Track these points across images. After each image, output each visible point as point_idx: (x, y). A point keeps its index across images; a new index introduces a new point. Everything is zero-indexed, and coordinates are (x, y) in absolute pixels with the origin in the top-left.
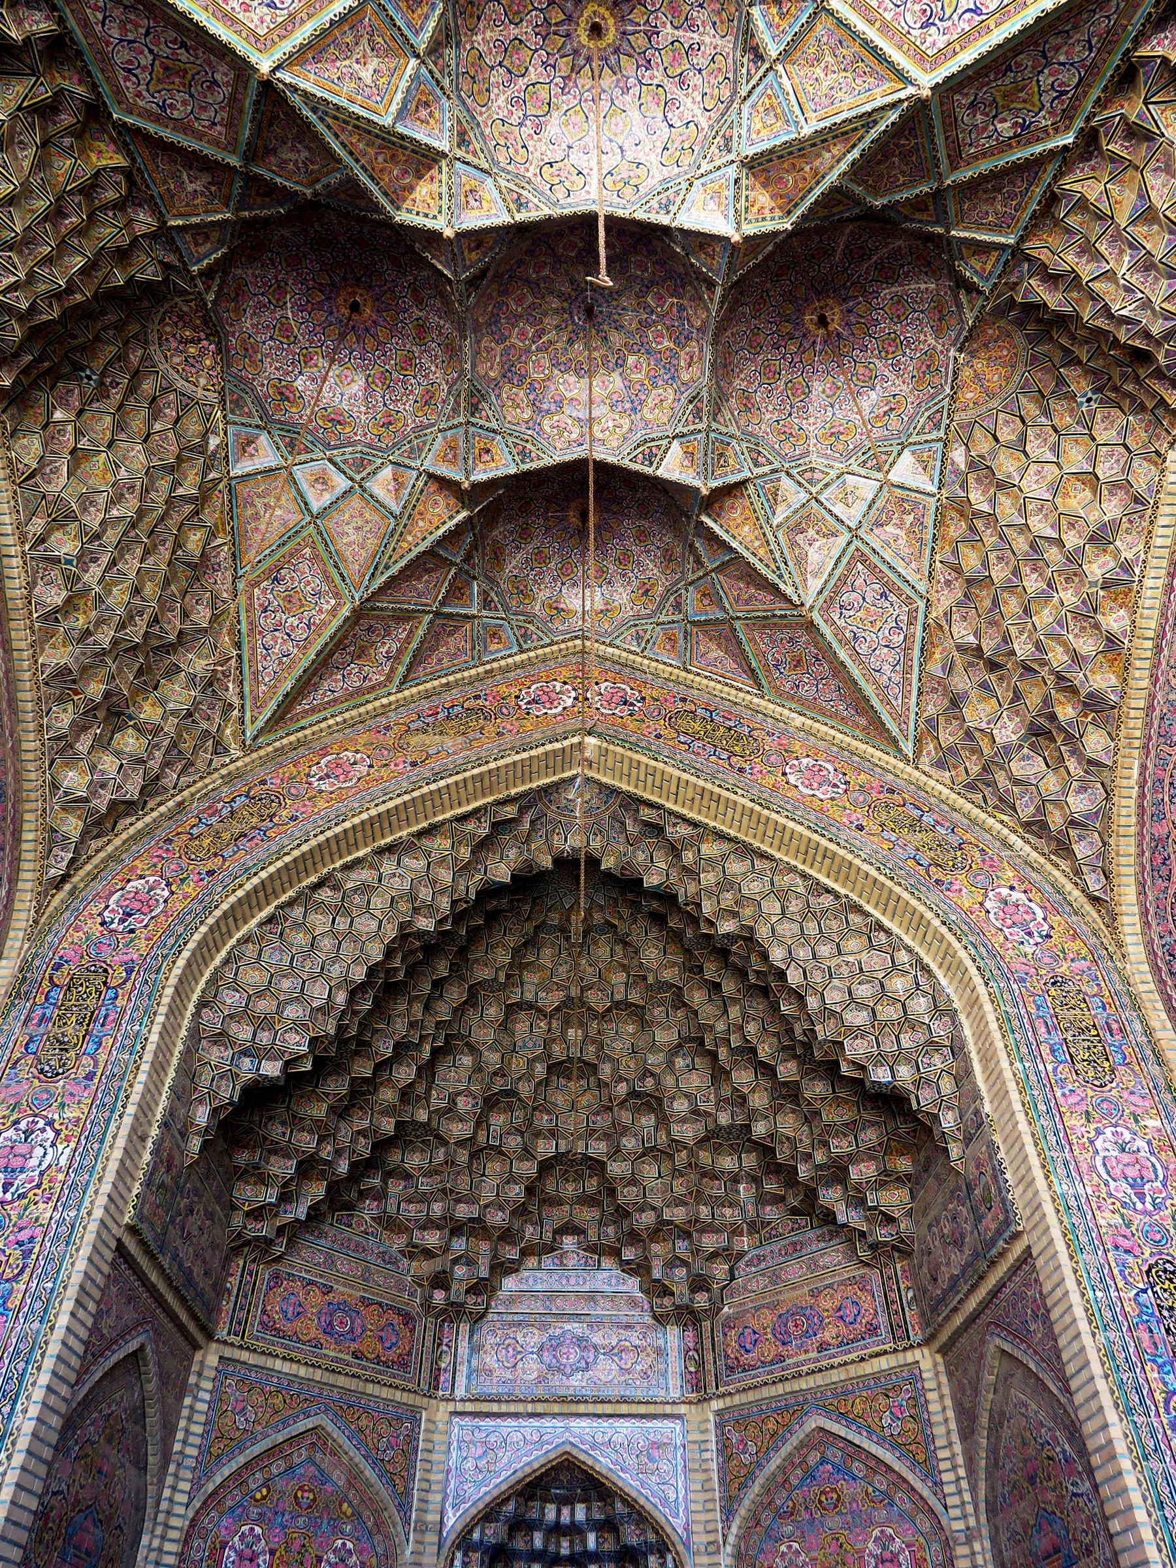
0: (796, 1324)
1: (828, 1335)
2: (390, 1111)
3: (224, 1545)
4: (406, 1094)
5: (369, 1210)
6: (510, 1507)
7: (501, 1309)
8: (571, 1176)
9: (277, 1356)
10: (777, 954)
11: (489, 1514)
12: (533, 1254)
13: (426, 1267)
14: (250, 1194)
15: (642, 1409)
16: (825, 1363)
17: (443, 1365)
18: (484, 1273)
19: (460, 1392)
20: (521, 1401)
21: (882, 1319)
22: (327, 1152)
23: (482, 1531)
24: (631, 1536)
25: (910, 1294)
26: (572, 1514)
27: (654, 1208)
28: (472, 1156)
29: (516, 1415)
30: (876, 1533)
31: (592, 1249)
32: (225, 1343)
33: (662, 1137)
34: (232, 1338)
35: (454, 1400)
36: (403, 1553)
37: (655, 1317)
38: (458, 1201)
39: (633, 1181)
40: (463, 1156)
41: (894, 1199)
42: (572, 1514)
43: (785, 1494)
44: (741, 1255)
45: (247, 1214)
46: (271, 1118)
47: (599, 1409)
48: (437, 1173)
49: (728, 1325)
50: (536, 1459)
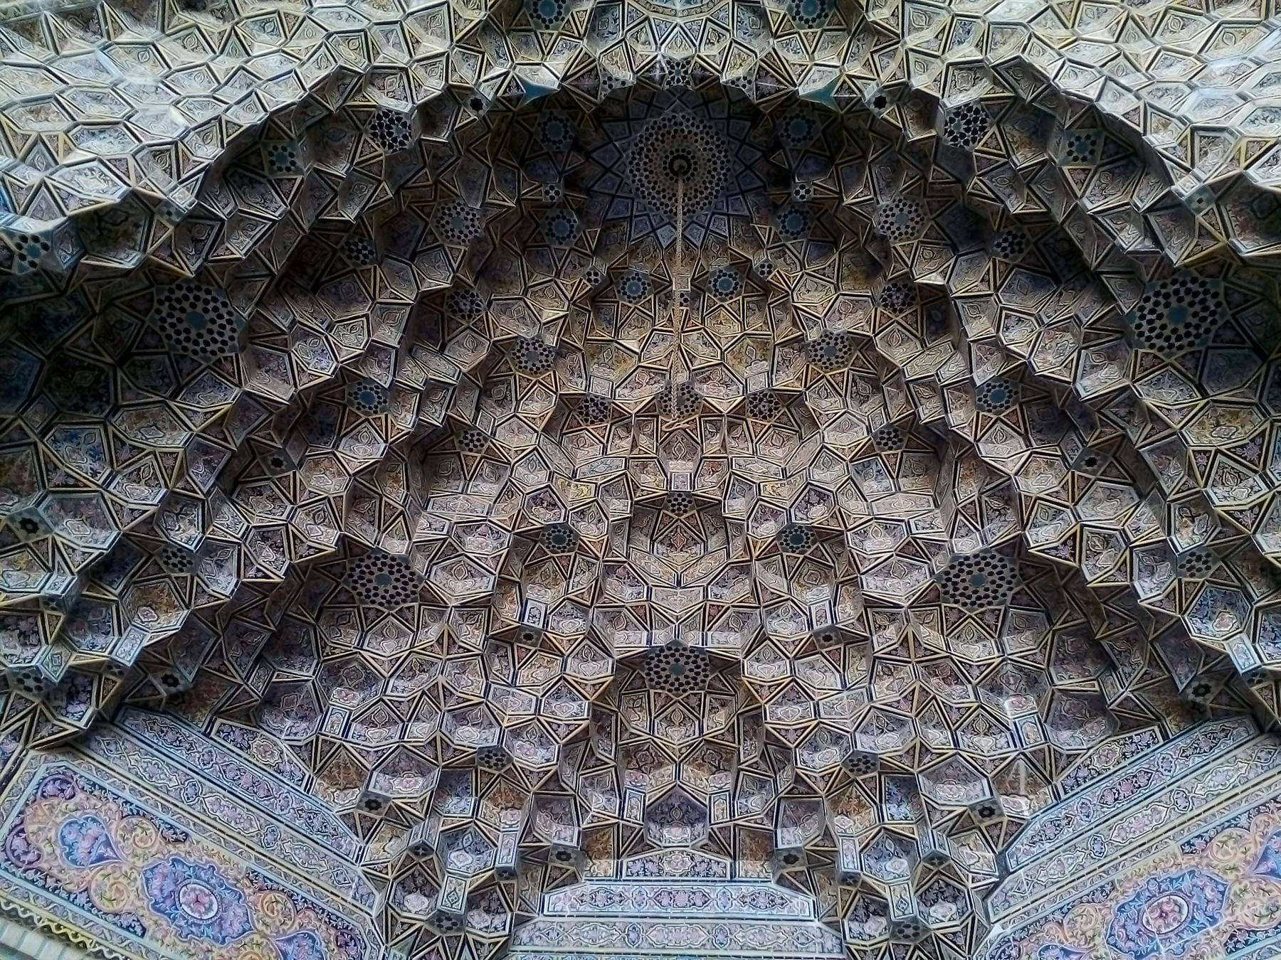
2: (324, 510)
4: (362, 492)
7: (540, 945)
8: (677, 712)
10: (1071, 84)
12: (604, 853)
33: (848, 612)
38: (461, 717)
40: (473, 637)
44: (1018, 826)
46: (72, 437)
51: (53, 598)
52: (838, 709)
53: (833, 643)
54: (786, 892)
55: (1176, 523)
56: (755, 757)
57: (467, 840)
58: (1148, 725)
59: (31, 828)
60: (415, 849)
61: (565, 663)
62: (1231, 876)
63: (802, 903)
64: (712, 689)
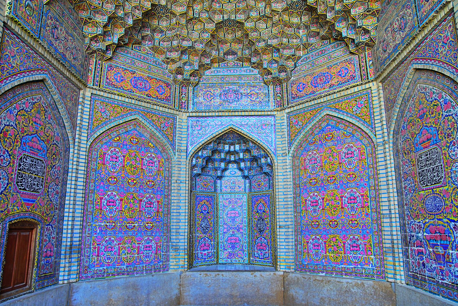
0: (321, 80)
1: (333, 82)
3: (105, 154)
5: (147, 45)
6: (212, 145)
8: (230, 31)
9: (115, 94)
11: (204, 147)
12: (215, 63)
13: (173, 67)
14: (90, 30)
15: (260, 113)
16: (331, 92)
17: (184, 101)
18: (197, 68)
19: (190, 110)
20: (213, 112)
21: (358, 74)
22: (121, 13)
23: (202, 153)
24: (255, 153)
25: (371, 62)
26: (235, 148)
27: (264, 41)
28: (188, 21)
29: (212, 116)
30: (347, 146)
31: (239, 60)
32: (92, 88)
33: (268, 10)
34: (95, 87)
35: (188, 112)
36: (173, 158)
37: (265, 83)
38: (183, 40)
39: (255, 30)
40: (183, 21)
41: (369, 23)
42: (235, 148)
43: (312, 137)
44: (299, 58)
45: (91, 39)
47: (243, 114)
48: (174, 29)
49: (293, 83)
50: (220, 130)
51: (100, 34)
52: (265, 34)
53: (265, 18)
54: (253, 69)
55: (336, 3)
56: (247, 43)
57: (188, 64)
58: (328, 39)
59: (109, 77)
60: (178, 68)
61: (204, 24)
62: (333, 74)
63: (256, 71)
64: (237, 27)
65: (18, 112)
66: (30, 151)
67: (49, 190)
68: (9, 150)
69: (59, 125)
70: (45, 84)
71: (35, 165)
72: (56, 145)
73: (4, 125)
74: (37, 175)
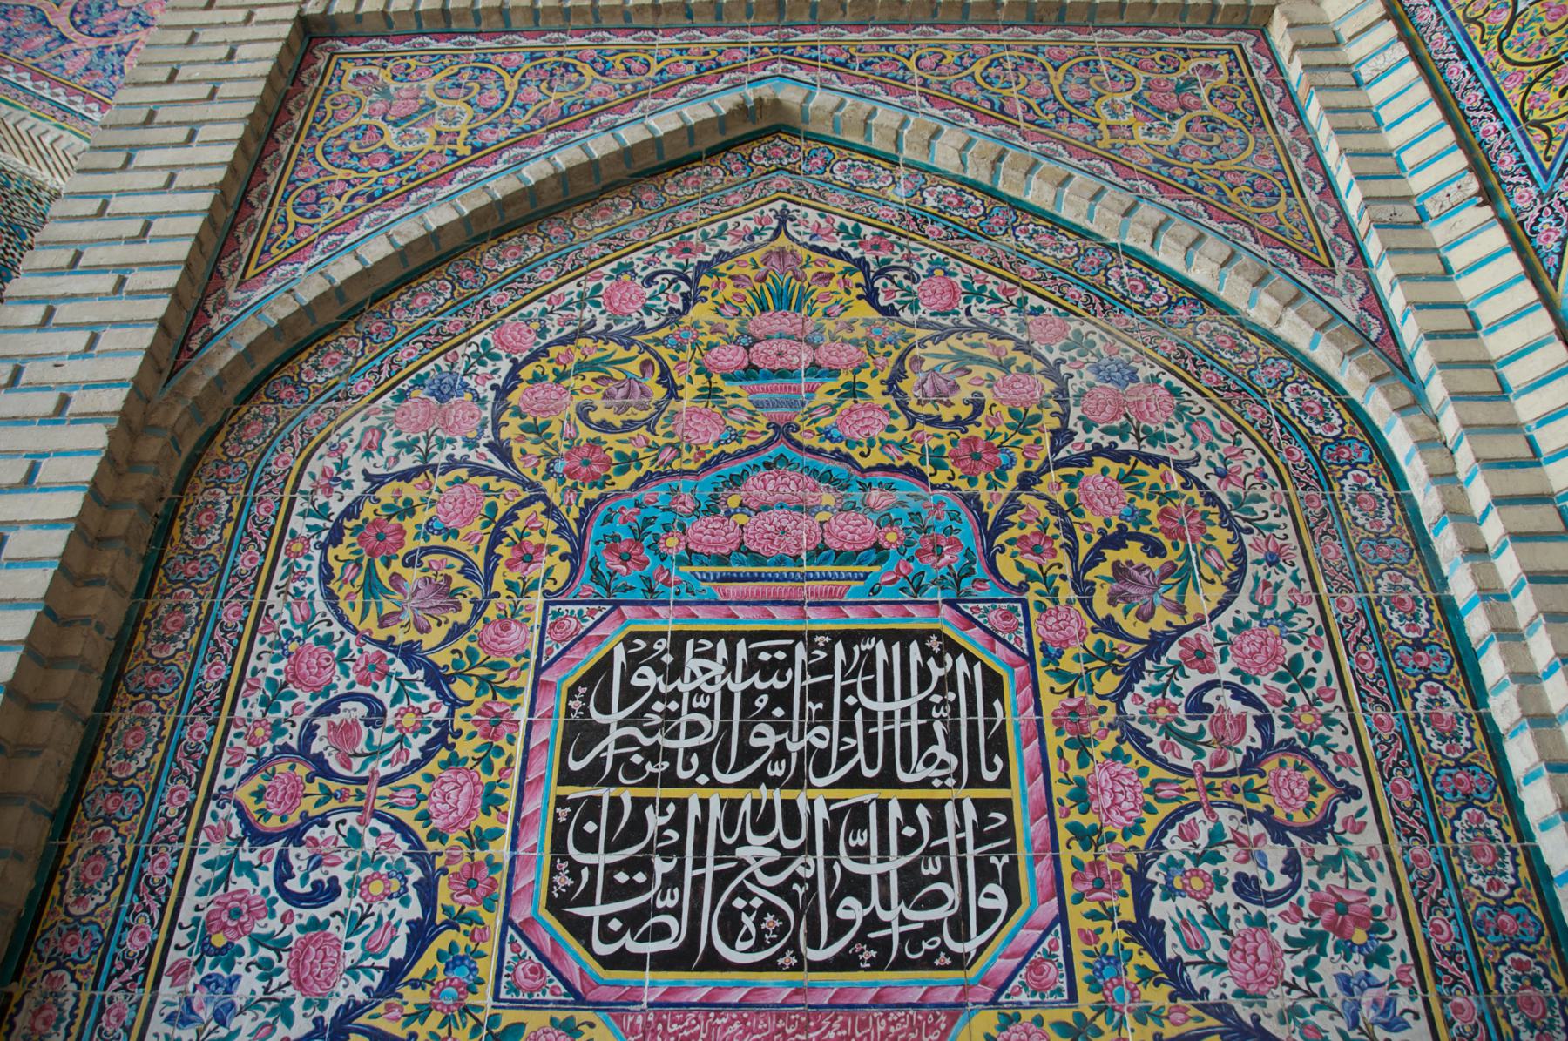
65: (517, 366)
66: (710, 589)
67: (1159, 908)
68: (429, 641)
69: (1102, 302)
70: (817, 138)
71: (821, 692)
72: (1122, 457)
73: (360, 485)
74: (887, 779)
